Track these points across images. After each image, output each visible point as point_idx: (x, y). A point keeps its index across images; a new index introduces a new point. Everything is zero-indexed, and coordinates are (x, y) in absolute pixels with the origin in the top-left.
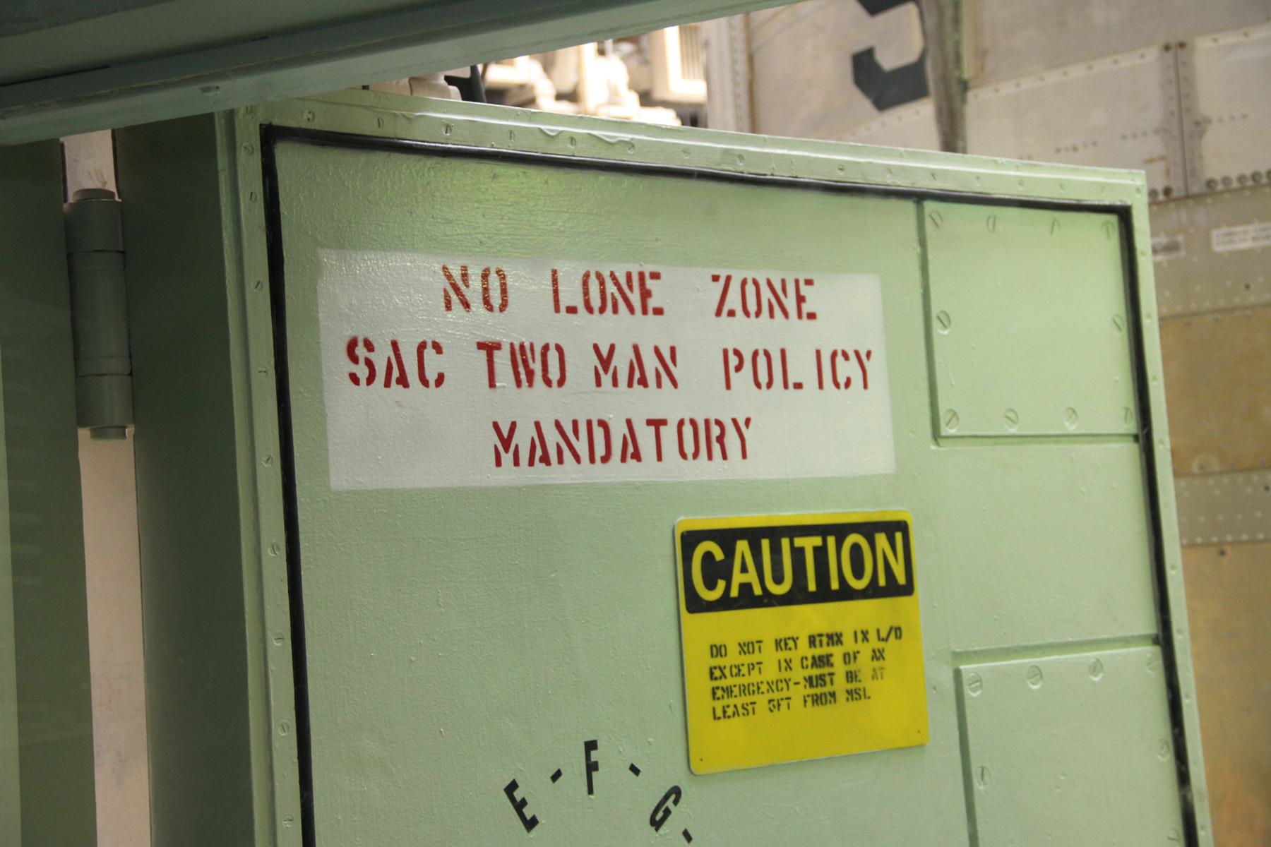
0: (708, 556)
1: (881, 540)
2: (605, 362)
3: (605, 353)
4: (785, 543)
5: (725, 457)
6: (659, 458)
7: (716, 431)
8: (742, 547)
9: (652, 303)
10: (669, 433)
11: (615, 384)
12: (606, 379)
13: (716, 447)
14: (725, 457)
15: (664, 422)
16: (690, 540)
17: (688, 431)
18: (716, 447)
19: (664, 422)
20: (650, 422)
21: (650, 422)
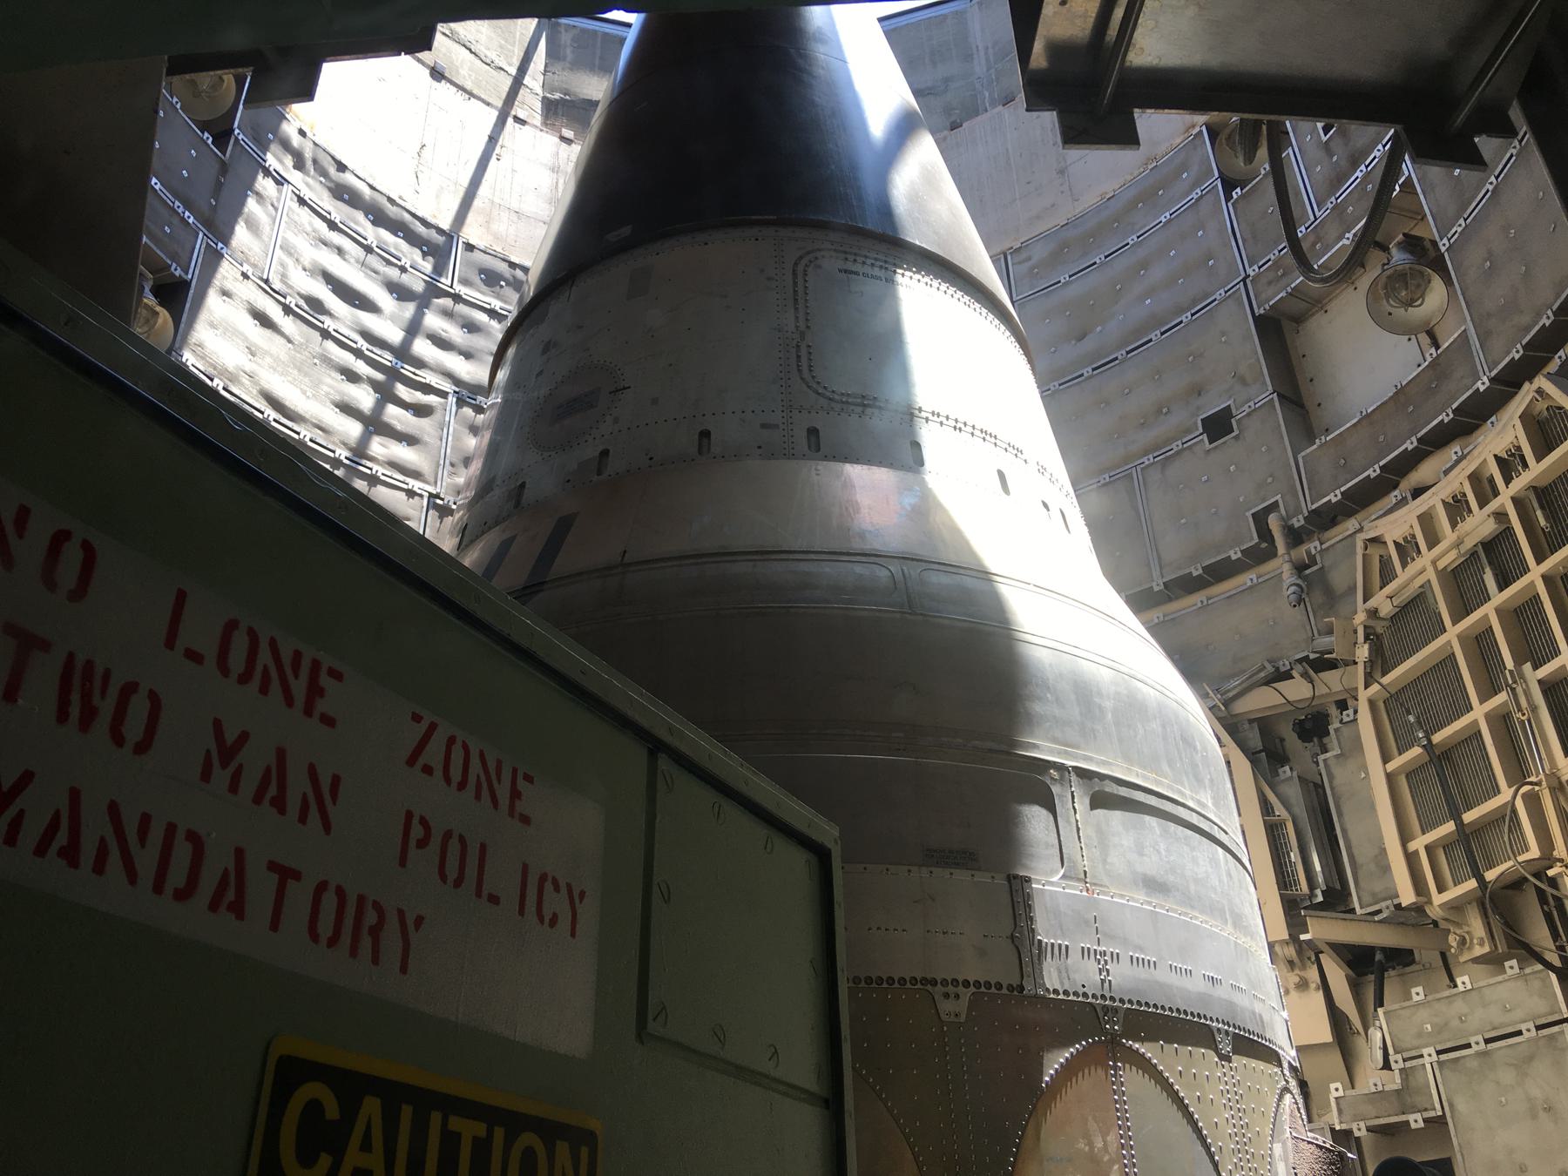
0: (314, 1107)
1: (562, 1149)
2: (228, 753)
3: (230, 736)
4: (436, 1118)
5: (375, 960)
6: (274, 926)
7: (371, 918)
8: (371, 1107)
9: (321, 706)
10: (299, 896)
11: (234, 787)
12: (221, 777)
13: (366, 942)
14: (375, 960)
15: (297, 876)
16: (292, 1072)
17: (329, 901)
18: (366, 942)
19: (297, 876)
20: (273, 866)
21: (273, 866)
